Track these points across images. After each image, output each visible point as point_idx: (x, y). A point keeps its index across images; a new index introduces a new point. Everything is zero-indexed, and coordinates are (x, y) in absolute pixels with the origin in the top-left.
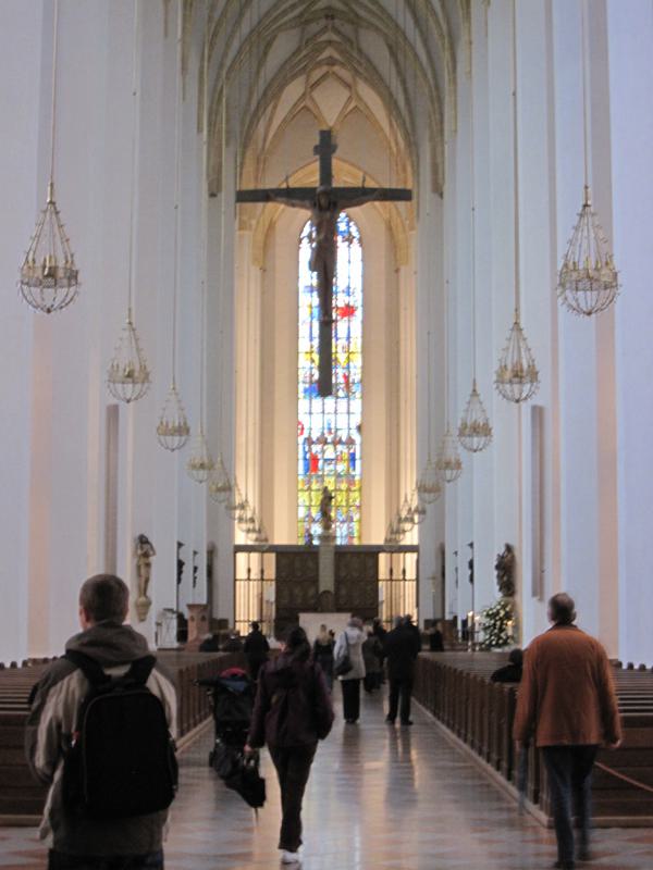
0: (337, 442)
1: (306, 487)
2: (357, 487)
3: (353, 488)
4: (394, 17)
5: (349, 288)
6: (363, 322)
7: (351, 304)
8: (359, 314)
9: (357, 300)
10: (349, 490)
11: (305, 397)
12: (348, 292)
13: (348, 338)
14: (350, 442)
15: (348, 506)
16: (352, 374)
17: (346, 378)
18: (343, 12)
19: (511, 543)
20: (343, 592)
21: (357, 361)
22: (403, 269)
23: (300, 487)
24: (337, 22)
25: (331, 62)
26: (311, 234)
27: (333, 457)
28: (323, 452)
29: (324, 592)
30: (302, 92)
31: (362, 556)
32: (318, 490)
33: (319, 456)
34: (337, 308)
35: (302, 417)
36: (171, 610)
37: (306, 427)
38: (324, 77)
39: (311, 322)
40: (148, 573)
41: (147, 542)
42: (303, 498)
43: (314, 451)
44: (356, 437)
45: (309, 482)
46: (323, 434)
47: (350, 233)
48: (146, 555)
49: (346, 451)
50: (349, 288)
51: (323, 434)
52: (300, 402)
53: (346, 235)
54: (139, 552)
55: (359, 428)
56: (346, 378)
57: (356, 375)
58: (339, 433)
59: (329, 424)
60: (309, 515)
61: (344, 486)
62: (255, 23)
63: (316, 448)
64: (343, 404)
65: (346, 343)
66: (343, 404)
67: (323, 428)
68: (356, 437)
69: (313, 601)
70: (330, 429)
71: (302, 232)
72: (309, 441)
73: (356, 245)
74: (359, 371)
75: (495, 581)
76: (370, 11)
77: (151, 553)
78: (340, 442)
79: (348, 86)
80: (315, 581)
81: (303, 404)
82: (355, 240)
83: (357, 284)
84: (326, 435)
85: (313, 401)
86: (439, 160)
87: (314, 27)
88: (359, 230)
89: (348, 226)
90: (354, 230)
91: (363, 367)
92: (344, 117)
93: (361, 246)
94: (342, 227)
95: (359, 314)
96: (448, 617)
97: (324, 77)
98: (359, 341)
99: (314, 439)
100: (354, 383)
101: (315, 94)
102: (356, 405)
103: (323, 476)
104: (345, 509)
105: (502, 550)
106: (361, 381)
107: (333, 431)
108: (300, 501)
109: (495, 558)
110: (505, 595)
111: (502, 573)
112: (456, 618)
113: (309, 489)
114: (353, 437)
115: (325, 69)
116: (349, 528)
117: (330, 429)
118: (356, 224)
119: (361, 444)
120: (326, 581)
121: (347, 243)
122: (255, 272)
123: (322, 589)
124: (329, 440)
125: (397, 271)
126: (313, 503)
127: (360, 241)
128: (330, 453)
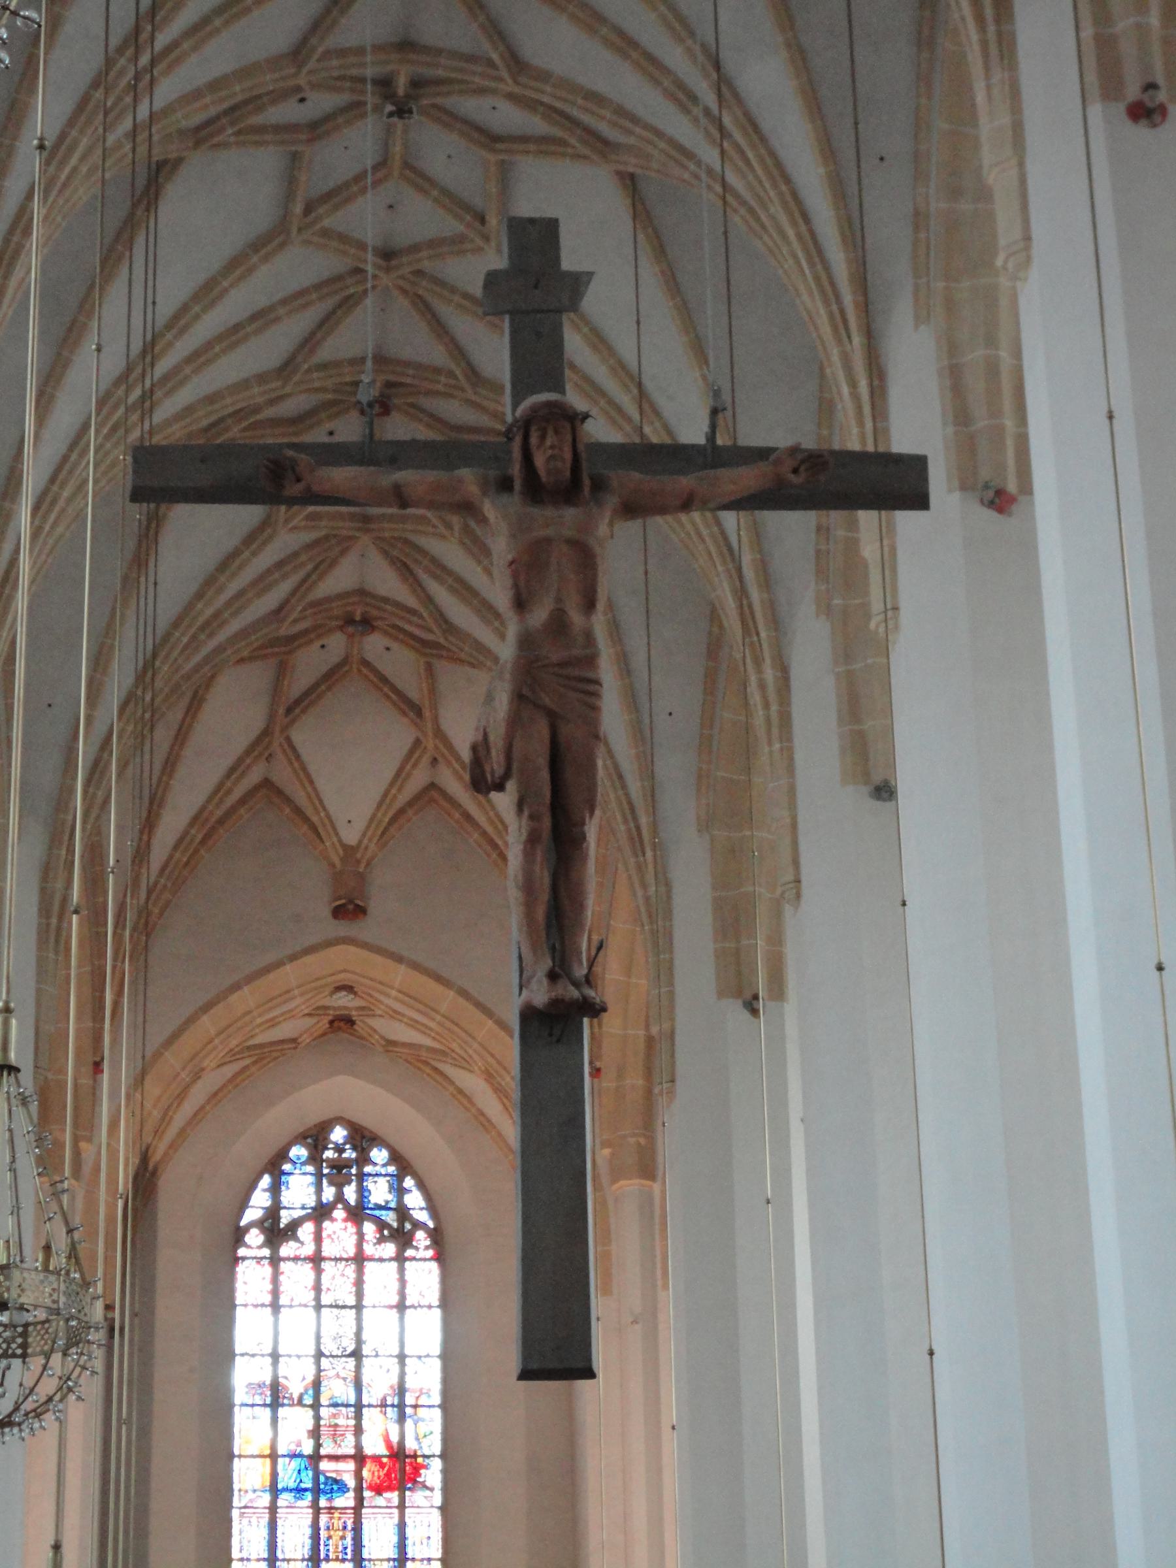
5: (401, 1390)
6: (443, 1509)
7: (411, 1445)
8: (433, 1475)
26: (273, 1213)
30: (258, 725)
34: (360, 1458)
39: (273, 1509)
47: (403, 1212)
50: (401, 1390)
53: (390, 1217)
62: (137, 346)
71: (244, 1204)
79: (411, 709)
82: (420, 1235)
88: (432, 1208)
89: (400, 1191)
90: (414, 1200)
93: (438, 1258)
94: (379, 1192)
97: (331, 677)
101: (304, 735)
115: (337, 644)
118: (421, 1185)
121: (390, 1249)
127: (437, 1237)
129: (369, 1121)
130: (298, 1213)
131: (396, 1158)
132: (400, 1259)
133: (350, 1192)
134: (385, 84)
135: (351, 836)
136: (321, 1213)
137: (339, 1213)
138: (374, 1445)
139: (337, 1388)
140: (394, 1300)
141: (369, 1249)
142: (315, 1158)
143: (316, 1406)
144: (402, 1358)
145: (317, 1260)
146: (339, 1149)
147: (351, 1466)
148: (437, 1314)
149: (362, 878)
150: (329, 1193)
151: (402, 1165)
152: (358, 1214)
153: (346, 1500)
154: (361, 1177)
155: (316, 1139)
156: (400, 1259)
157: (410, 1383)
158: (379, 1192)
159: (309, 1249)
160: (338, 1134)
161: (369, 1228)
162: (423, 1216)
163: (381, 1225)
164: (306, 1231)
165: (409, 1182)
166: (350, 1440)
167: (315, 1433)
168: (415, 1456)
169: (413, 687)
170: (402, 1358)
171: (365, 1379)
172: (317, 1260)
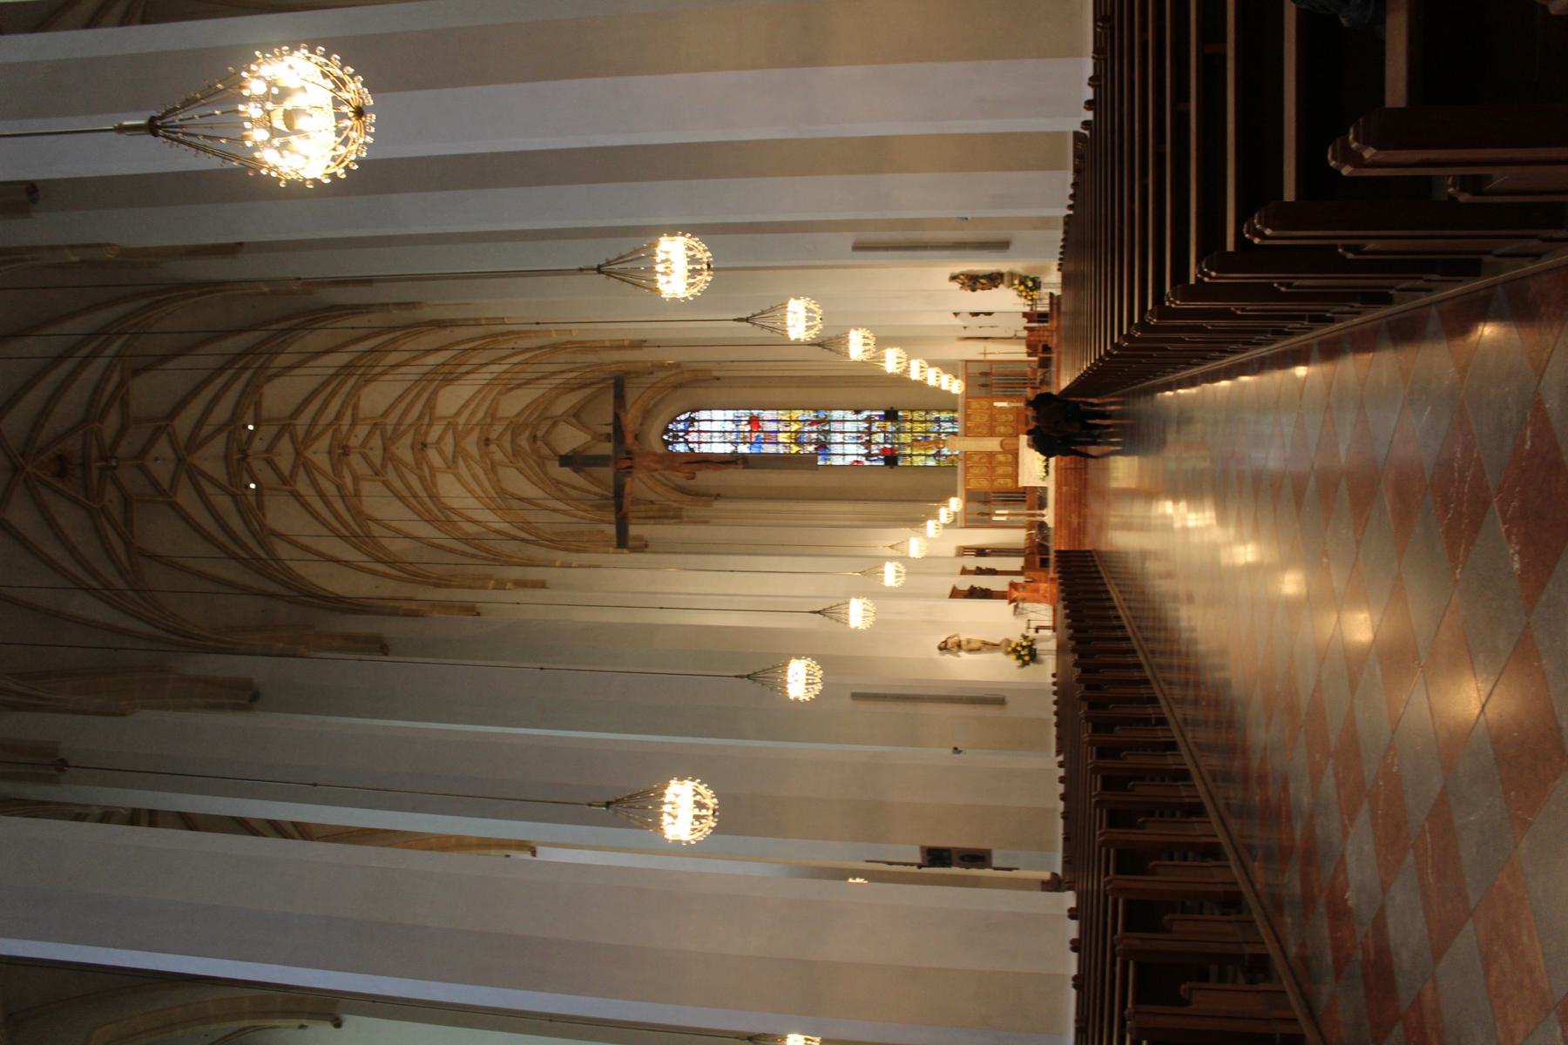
0: (869, 432)
1: (909, 459)
2: (908, 413)
3: (909, 418)
4: (477, 388)
6: (764, 410)
7: (747, 418)
8: (755, 412)
9: (744, 414)
10: (911, 421)
11: (829, 460)
12: (736, 421)
13: (778, 421)
14: (869, 420)
15: (925, 421)
16: (809, 418)
17: (813, 423)
18: (481, 429)
19: (948, 277)
20: (1002, 429)
21: (797, 414)
22: (716, 374)
23: (908, 464)
24: (493, 436)
25: (534, 438)
27: (882, 435)
28: (878, 443)
29: (1001, 445)
31: (969, 411)
32: (912, 449)
33: (882, 446)
34: (750, 431)
35: (849, 460)
36: (1016, 607)
37: (855, 458)
38: (547, 444)
40: (976, 641)
41: (945, 642)
42: (918, 461)
43: (877, 452)
44: (865, 414)
45: (905, 455)
46: (861, 444)
47: (686, 420)
48: (959, 645)
49: (877, 424)
51: (861, 444)
52: (834, 464)
54: (955, 649)
55: (857, 412)
56: (813, 423)
57: (811, 415)
58: (861, 429)
59: (854, 438)
60: (934, 456)
61: (908, 425)
63: (875, 450)
64: (836, 426)
65: (782, 423)
66: (836, 426)
67: (857, 443)
68: (865, 414)
69: (1010, 457)
70: (858, 438)
72: (868, 456)
73: (697, 415)
74: (806, 412)
75: (987, 292)
76: (478, 406)
77: (956, 638)
78: (869, 428)
79: (555, 424)
80: (991, 455)
81: (837, 461)
83: (730, 414)
84: (863, 441)
85: (832, 452)
86: (607, 344)
87: (498, 456)
89: (681, 421)
90: (683, 417)
91: (804, 410)
92: (584, 427)
93: (698, 411)
94: (681, 426)
95: (755, 412)
96: (1025, 333)
97: (547, 444)
98: (780, 412)
99: (866, 451)
100: (817, 417)
102: (836, 414)
103: (898, 444)
104: (929, 424)
105: (956, 286)
106: (816, 410)
107: (859, 435)
108: (920, 464)
109: (963, 291)
110: (1002, 282)
111: (979, 285)
112: (1026, 328)
113: (911, 455)
114: (865, 417)
116: (945, 421)
117: (858, 438)
118: (678, 416)
119: (872, 410)
120: (993, 444)
122: (718, 505)
123: (1000, 450)
124: (868, 438)
125: (718, 379)
126: (923, 452)
128: (879, 438)
129: (661, 429)
130: (687, 448)
131: (671, 423)
132: (698, 421)
133: (681, 434)
134: (422, 449)
135: (589, 438)
136: (687, 442)
137: (687, 437)
138: (748, 428)
139: (733, 437)
140: (709, 422)
141: (696, 429)
142: (672, 443)
143: (737, 443)
144: (725, 420)
145: (699, 443)
146: (669, 437)
147: (754, 435)
148: (713, 411)
149: (601, 435)
150: (681, 440)
151: (674, 420)
152: (687, 432)
153: (762, 436)
154: (677, 431)
155: (667, 443)
156: (698, 421)
157: (732, 418)
158: (681, 426)
159: (696, 445)
160: (665, 437)
161: (690, 429)
162: (687, 415)
163: (690, 426)
164: (691, 445)
165: (678, 419)
166: (746, 434)
167: (745, 443)
168: (751, 417)
169: (550, 422)
170: (725, 420)
171: (730, 430)
172: (699, 443)
